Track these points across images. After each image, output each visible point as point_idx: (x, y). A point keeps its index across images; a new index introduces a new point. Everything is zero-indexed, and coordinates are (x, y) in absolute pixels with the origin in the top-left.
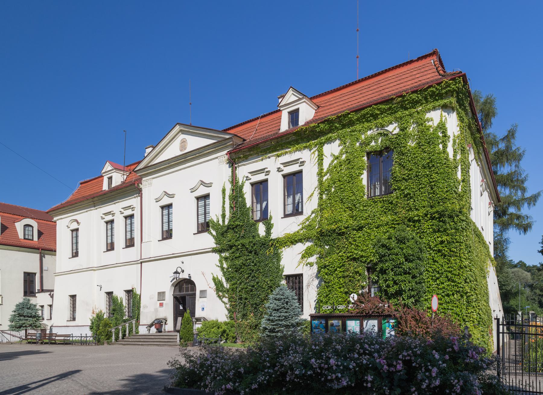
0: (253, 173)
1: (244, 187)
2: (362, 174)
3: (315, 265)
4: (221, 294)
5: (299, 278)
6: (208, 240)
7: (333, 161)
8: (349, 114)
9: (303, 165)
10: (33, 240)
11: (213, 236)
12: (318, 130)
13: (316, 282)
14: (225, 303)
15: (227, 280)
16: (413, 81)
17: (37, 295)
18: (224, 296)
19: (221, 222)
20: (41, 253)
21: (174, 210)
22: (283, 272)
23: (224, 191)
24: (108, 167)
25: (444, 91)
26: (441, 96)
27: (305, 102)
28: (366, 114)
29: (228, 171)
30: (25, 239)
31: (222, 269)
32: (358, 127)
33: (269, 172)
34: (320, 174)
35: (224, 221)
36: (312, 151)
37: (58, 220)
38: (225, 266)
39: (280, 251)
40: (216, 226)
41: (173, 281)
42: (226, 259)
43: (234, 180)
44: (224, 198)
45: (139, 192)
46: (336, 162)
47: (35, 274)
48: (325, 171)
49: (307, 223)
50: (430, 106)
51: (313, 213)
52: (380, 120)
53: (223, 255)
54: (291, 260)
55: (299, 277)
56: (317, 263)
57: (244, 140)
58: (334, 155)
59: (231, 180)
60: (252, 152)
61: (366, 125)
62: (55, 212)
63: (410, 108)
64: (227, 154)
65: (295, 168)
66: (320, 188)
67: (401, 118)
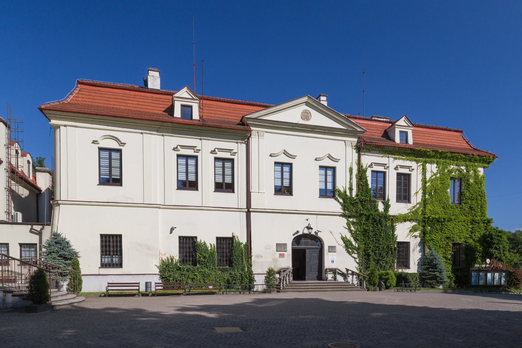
7: (432, 176)
11: (340, 203)
13: (419, 248)
14: (355, 258)
15: (356, 240)
19: (348, 193)
23: (351, 170)
28: (454, 155)
29: (356, 155)
31: (351, 231)
32: (448, 161)
34: (424, 182)
36: (419, 164)
38: (352, 228)
40: (343, 195)
41: (296, 235)
42: (353, 223)
46: (434, 177)
48: (427, 180)
49: (414, 210)
50: (480, 164)
53: (351, 220)
55: (407, 244)
61: (452, 162)
62: (80, 115)
65: (406, 171)
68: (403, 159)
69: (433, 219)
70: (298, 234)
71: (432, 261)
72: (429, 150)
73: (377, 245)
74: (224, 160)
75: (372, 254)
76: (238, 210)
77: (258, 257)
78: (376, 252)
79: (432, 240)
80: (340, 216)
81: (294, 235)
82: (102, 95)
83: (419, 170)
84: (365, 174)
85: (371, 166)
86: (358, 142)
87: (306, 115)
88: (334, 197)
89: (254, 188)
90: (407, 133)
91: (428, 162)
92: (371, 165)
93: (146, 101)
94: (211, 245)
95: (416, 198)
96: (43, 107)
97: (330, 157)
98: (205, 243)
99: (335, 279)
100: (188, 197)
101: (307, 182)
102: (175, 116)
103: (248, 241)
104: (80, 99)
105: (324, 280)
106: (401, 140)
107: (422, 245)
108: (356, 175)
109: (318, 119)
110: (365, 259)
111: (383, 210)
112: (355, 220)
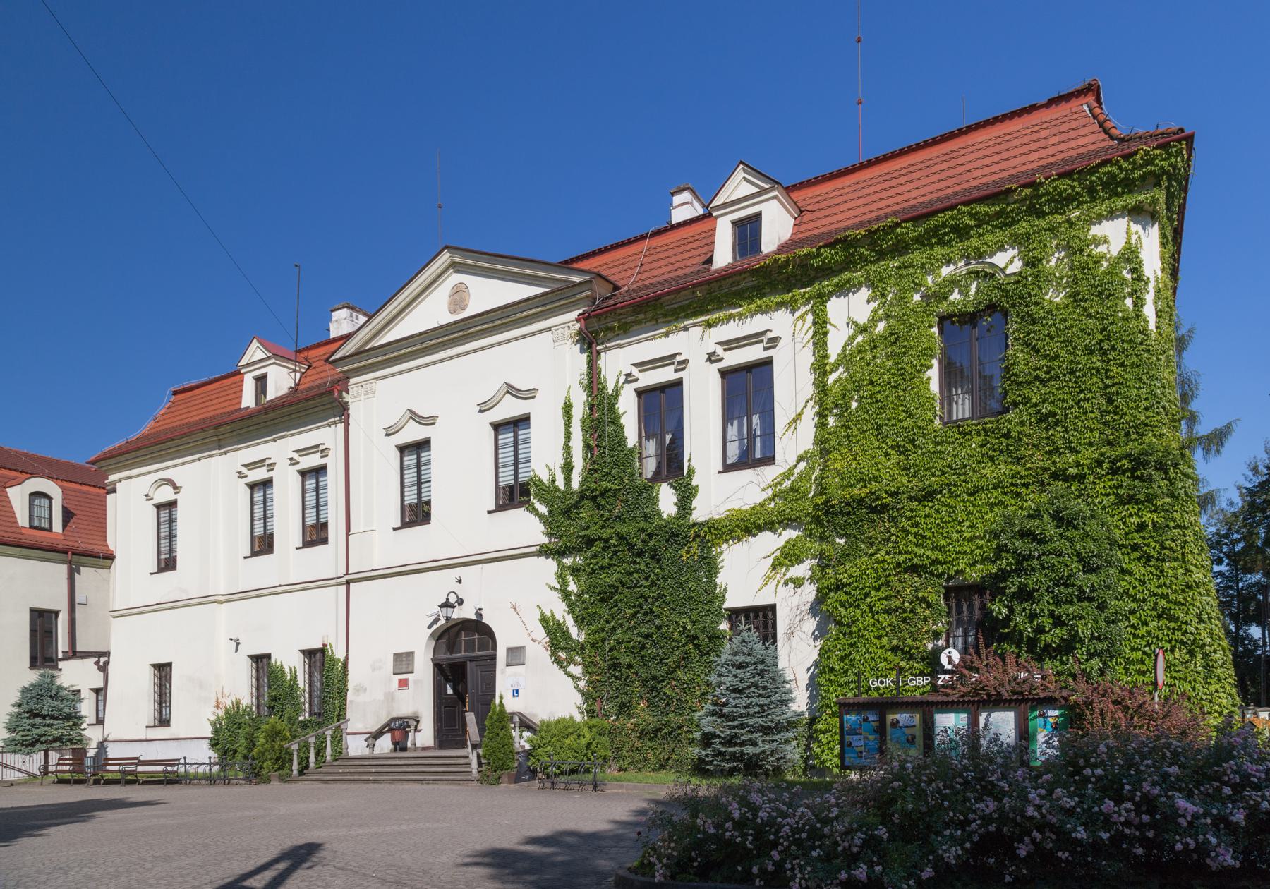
0: (644, 365)
1: (620, 399)
2: (930, 367)
3: (807, 583)
4: (562, 655)
5: (765, 616)
6: (526, 527)
7: (853, 338)
8: (897, 225)
9: (774, 347)
10: (50, 530)
11: (541, 516)
12: (816, 262)
13: (811, 624)
15: (579, 621)
16: (1044, 153)
17: (61, 665)
18: (571, 661)
19: (560, 483)
20: (70, 562)
21: (435, 454)
22: (724, 600)
23: (568, 409)
24: (256, 352)
25: (1137, 174)
26: (1129, 186)
27: (775, 197)
28: (939, 226)
30: (31, 527)
31: (566, 594)
32: (918, 257)
33: (685, 362)
34: (821, 368)
35: (568, 480)
36: (798, 314)
37: (120, 480)
38: (573, 587)
39: (714, 551)
40: (547, 492)
41: (435, 627)
42: (575, 571)
43: (593, 381)
44: (568, 425)
45: (341, 411)
47: (57, 613)
48: (832, 360)
49: (787, 484)
50: (1102, 208)
51: (800, 459)
52: (974, 242)
53: (568, 561)
54: (743, 573)
57: (616, 288)
58: (856, 324)
59: (585, 382)
60: (641, 316)
61: (938, 251)
62: (113, 461)
63: (1051, 213)
64: (578, 320)
65: (753, 353)
66: (821, 402)
67: (1028, 237)
81: (429, 627)
83: (799, 336)
91: (830, 294)
95: (795, 439)
100: (265, 570)
108: (583, 421)
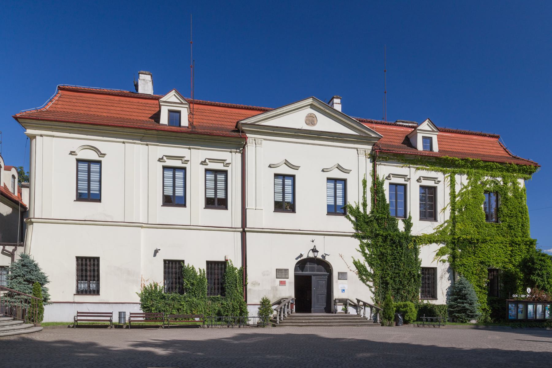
11: (352, 221)
13: (448, 275)
14: (370, 287)
15: (371, 265)
19: (361, 210)
22: (420, 264)
23: (365, 183)
29: (370, 165)
32: (481, 171)
34: (453, 195)
35: (365, 209)
36: (446, 176)
38: (367, 251)
40: (356, 213)
41: (299, 259)
42: (368, 245)
46: (465, 190)
48: (457, 193)
49: (441, 229)
50: (520, 175)
52: (494, 173)
53: (365, 241)
55: (434, 270)
56: (448, 261)
65: (431, 183)
68: (427, 170)
69: (464, 240)
70: (302, 258)
71: (461, 290)
72: (457, 159)
73: (397, 271)
74: (216, 172)
75: (391, 282)
76: (232, 229)
77: (254, 284)
78: (396, 279)
79: (463, 265)
80: (352, 236)
81: (297, 259)
82: (84, 102)
83: (446, 183)
84: (382, 188)
85: (388, 177)
86: (373, 150)
87: (311, 120)
88: (344, 214)
89: (250, 205)
90: (431, 138)
91: (457, 173)
92: (389, 176)
93: (131, 106)
94: (200, 270)
95: (444, 215)
96: (18, 115)
97: (339, 167)
98: (193, 268)
99: (346, 311)
100: (174, 214)
101: (312, 196)
102: (161, 122)
103: (243, 266)
104: (59, 106)
105: (333, 313)
106: (424, 147)
107: (452, 271)
108: (371, 189)
109: (325, 124)
110: (383, 288)
111: (404, 230)
112: (369, 242)
